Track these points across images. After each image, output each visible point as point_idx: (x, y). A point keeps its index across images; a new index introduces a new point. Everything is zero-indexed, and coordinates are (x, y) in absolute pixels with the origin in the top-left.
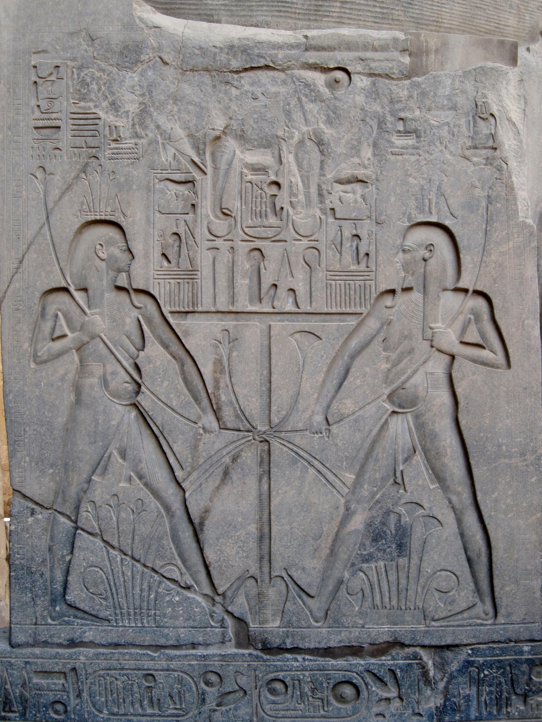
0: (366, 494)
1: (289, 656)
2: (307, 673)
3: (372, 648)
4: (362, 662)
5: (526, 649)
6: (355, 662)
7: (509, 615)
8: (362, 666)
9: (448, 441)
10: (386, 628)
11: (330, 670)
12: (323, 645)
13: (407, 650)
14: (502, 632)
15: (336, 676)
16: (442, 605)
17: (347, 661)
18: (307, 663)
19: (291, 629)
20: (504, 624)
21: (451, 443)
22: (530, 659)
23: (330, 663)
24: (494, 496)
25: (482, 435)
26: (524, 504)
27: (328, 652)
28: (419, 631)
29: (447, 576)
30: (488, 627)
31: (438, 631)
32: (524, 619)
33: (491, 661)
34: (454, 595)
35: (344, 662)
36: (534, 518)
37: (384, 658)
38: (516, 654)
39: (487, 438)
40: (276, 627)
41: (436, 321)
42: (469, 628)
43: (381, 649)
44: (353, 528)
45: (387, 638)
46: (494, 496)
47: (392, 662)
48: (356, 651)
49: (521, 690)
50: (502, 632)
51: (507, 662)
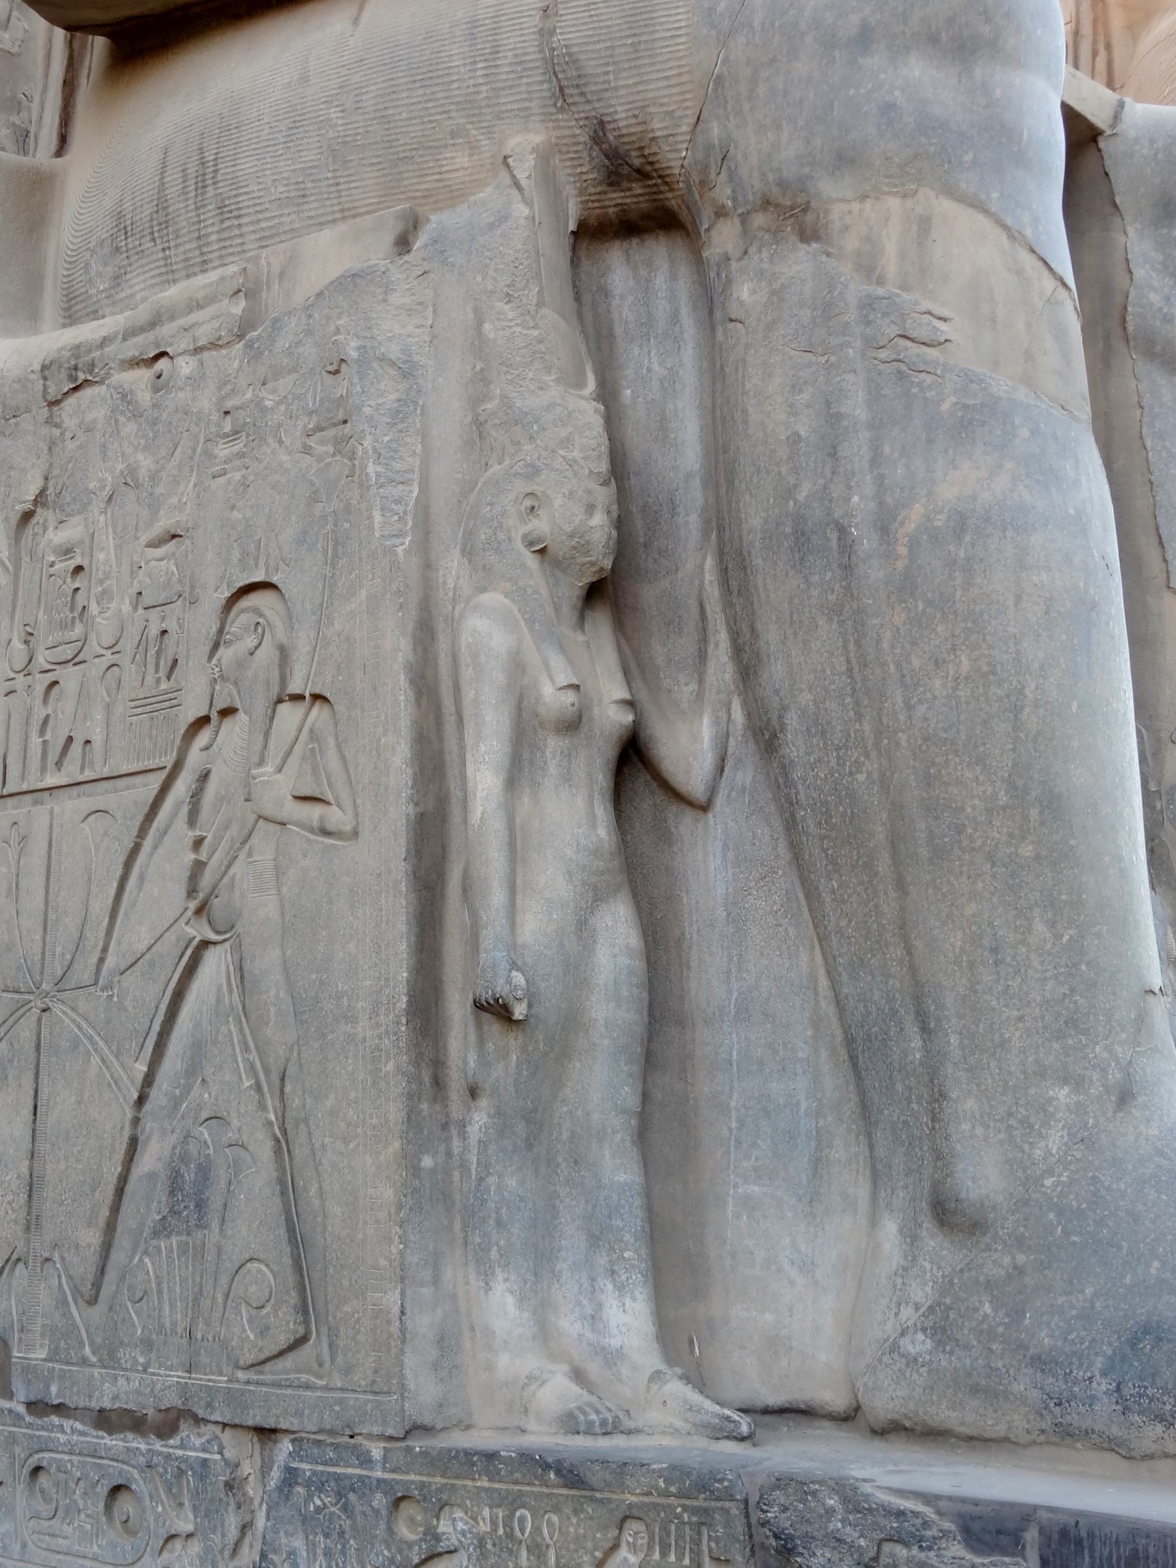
0: (164, 1102)
1: (55, 1420)
2: (75, 1459)
3: (162, 1416)
4: (143, 1447)
5: (376, 1451)
6: (134, 1445)
7: (347, 1371)
8: (143, 1455)
9: (272, 993)
10: (177, 1376)
11: (102, 1458)
12: (95, 1404)
13: (203, 1429)
14: (337, 1408)
15: (111, 1470)
16: (252, 1337)
17: (123, 1440)
18: (75, 1437)
19: (57, 1366)
20: (342, 1389)
21: (277, 995)
22: (385, 1481)
23: (103, 1441)
24: (328, 1104)
25: (314, 976)
26: (375, 1121)
27: (105, 1420)
28: (218, 1389)
29: (259, 1271)
30: (319, 1394)
31: (243, 1392)
32: (373, 1382)
33: (322, 1472)
34: (268, 1314)
35: (121, 1443)
36: (390, 1150)
37: (171, 1442)
38: (360, 1466)
39: (322, 983)
40: (42, 1360)
41: (261, 762)
42: (289, 1392)
43: (168, 1424)
44: (146, 1169)
45: (172, 1400)
46: (328, 1104)
47: (180, 1452)
48: (135, 1423)
49: (377, 1555)
50: (337, 1408)
51: (347, 1482)
